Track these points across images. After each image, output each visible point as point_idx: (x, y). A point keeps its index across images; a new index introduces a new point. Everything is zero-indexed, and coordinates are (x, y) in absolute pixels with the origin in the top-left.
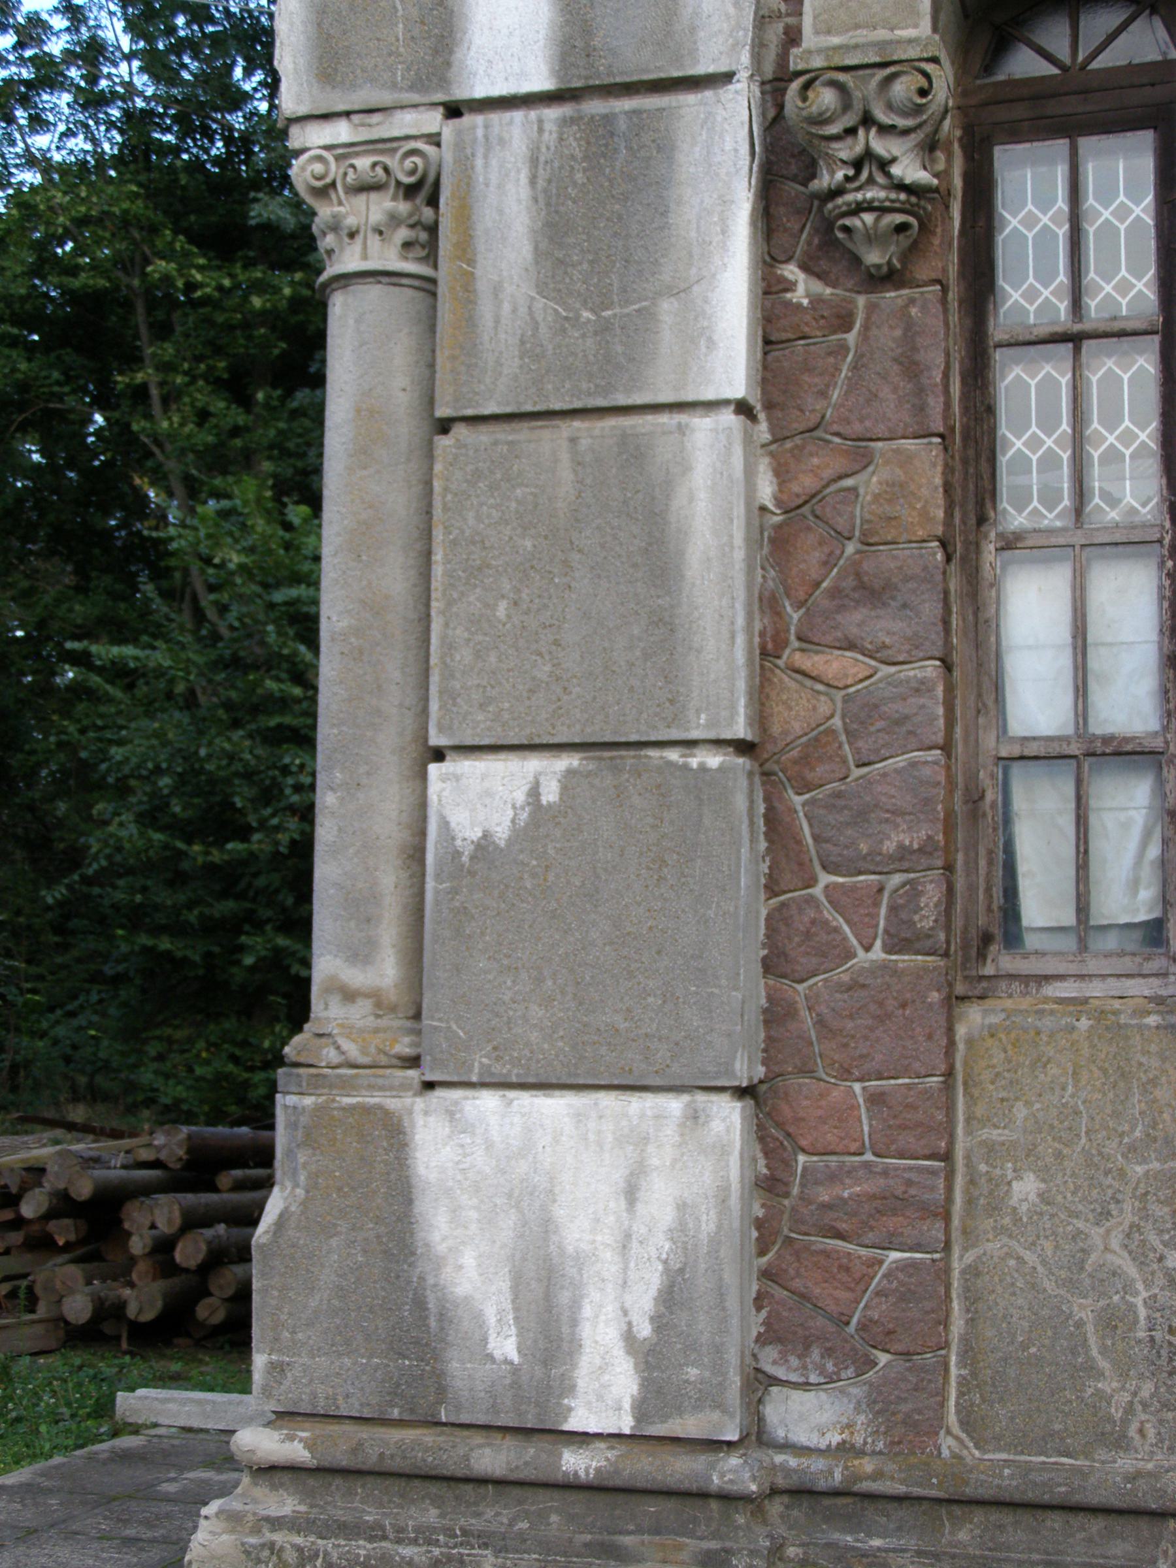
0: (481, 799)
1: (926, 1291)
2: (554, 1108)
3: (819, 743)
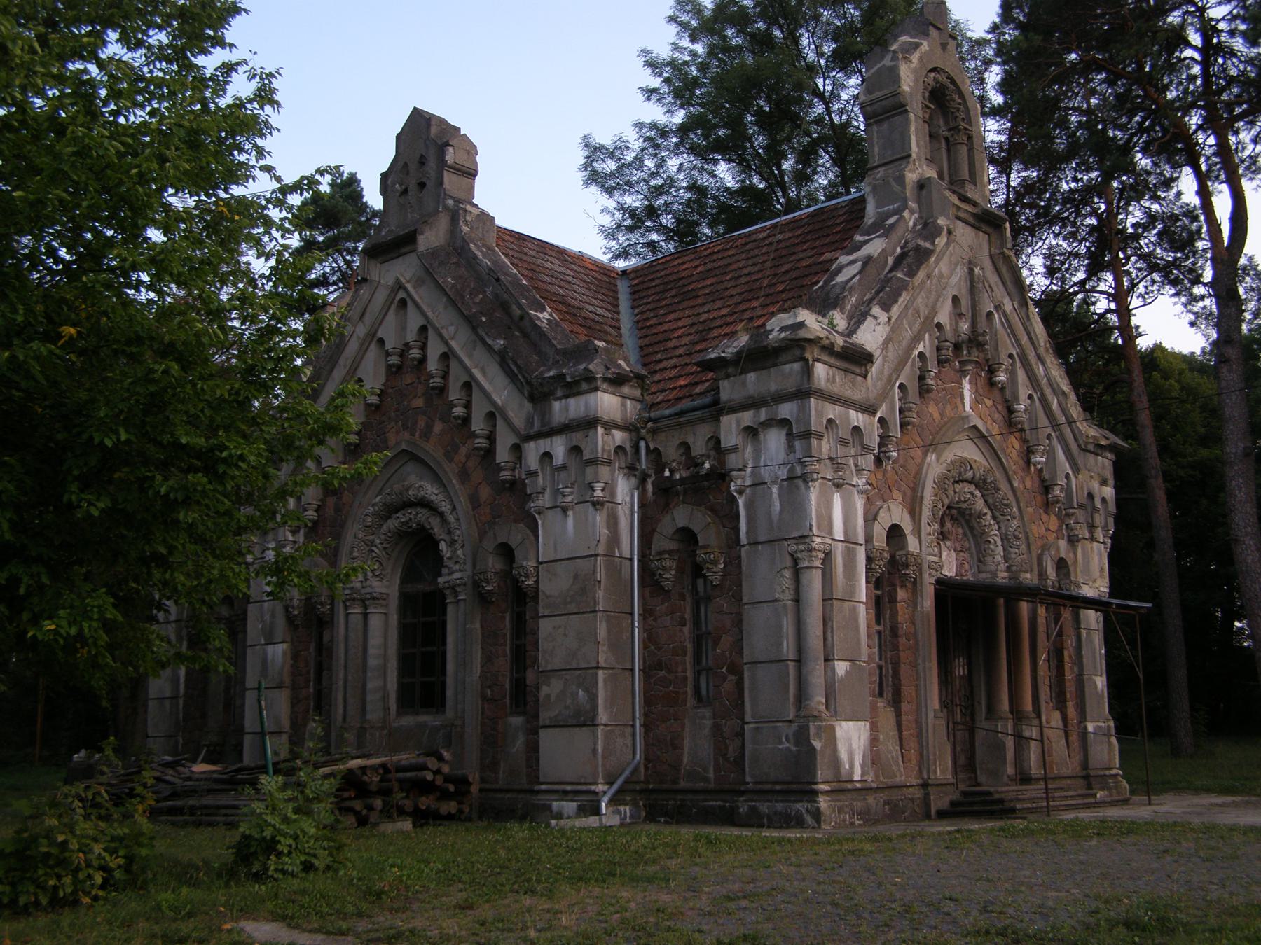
2: (851, 723)
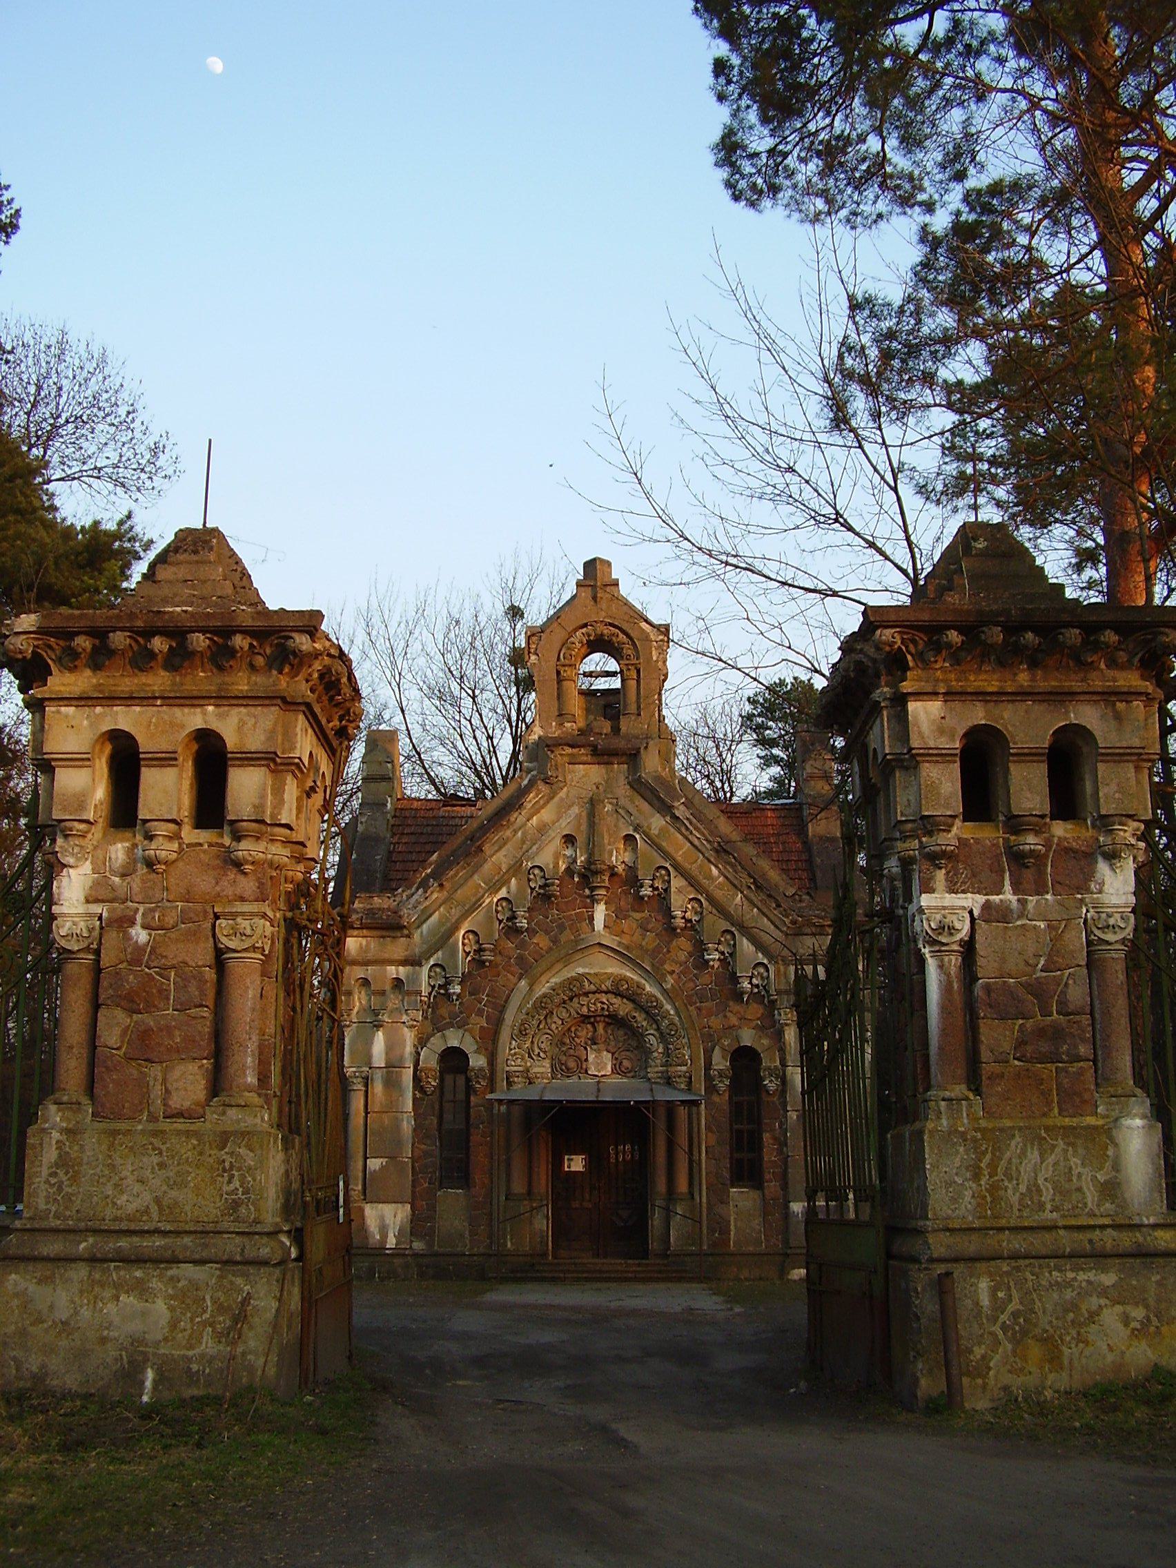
0: (374, 1164)
1: (432, 1228)
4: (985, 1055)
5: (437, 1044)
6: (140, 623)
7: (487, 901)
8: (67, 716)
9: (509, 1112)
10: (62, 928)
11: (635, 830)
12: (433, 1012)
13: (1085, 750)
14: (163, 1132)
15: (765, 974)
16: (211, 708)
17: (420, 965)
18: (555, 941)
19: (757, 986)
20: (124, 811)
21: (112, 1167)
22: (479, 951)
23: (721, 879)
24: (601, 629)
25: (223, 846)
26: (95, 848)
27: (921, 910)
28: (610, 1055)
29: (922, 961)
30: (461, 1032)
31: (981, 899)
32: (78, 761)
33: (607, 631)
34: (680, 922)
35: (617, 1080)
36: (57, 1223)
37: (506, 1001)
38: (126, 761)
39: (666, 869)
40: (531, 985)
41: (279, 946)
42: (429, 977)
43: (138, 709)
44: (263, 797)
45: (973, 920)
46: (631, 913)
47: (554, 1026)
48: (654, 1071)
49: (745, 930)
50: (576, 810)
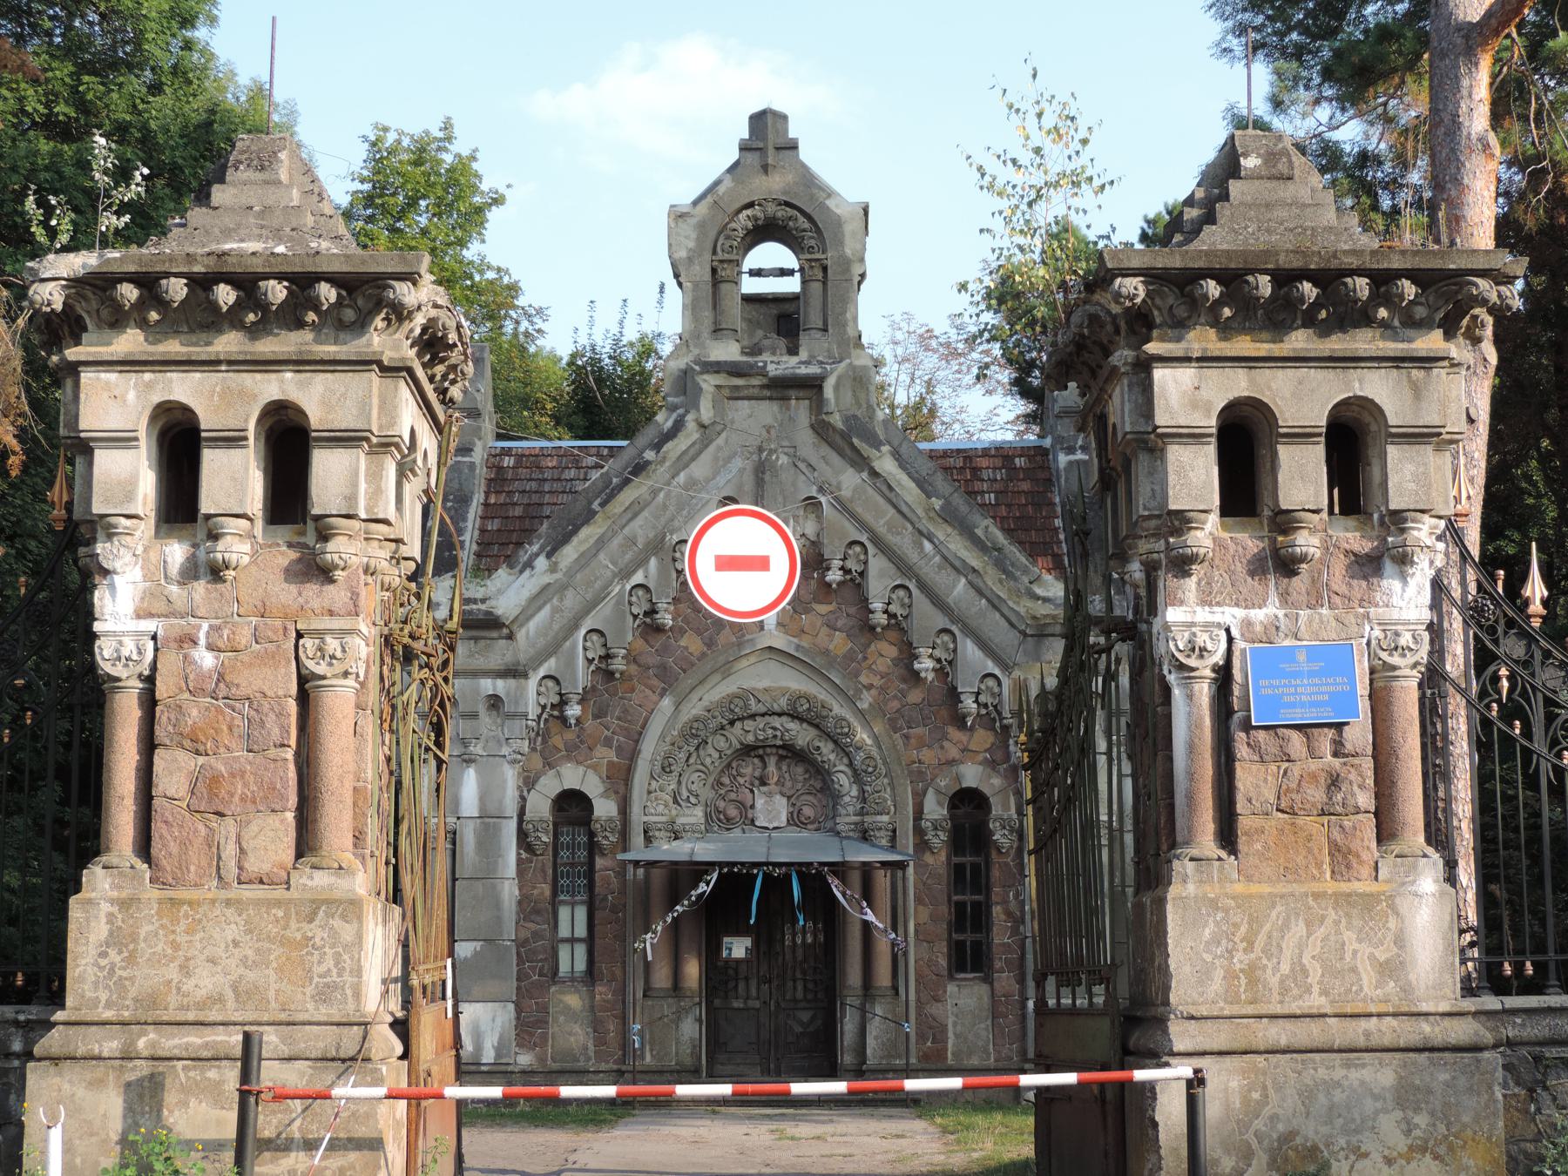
1: (544, 1037)
3: (526, 941)
4: (1241, 806)
5: (548, 787)
6: (198, 268)
7: (617, 590)
8: (107, 383)
9: (647, 875)
10: (104, 650)
11: (821, 490)
12: (544, 742)
13: (1374, 427)
14: (239, 901)
15: (996, 690)
16: (289, 375)
17: (525, 676)
18: (710, 644)
19: (986, 706)
20: (180, 503)
21: (176, 946)
22: (607, 657)
23: (938, 558)
24: (771, 209)
25: (305, 546)
26: (146, 550)
27: (1167, 627)
28: (784, 800)
29: (1167, 691)
30: (581, 769)
31: (1240, 613)
32: (123, 441)
33: (782, 213)
34: (881, 619)
35: (794, 834)
36: (108, 1015)
37: (643, 727)
38: (180, 444)
39: (862, 544)
40: (678, 705)
41: (375, 669)
42: (539, 694)
43: (198, 375)
44: (355, 485)
45: (1230, 640)
46: (816, 606)
47: (708, 761)
48: (847, 818)
49: (970, 632)
50: (738, 463)
